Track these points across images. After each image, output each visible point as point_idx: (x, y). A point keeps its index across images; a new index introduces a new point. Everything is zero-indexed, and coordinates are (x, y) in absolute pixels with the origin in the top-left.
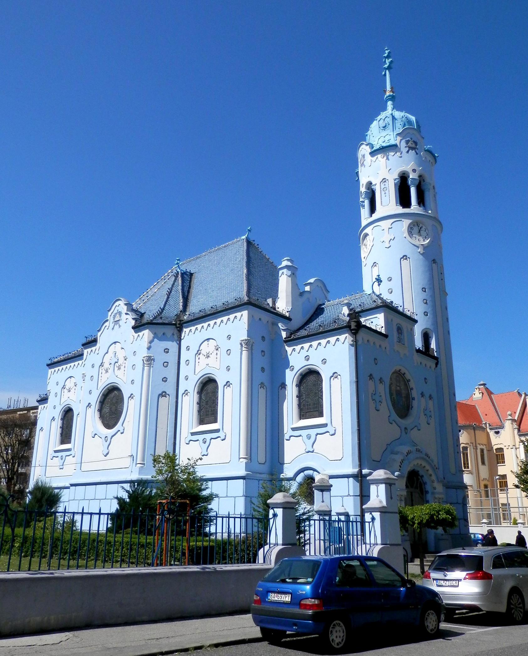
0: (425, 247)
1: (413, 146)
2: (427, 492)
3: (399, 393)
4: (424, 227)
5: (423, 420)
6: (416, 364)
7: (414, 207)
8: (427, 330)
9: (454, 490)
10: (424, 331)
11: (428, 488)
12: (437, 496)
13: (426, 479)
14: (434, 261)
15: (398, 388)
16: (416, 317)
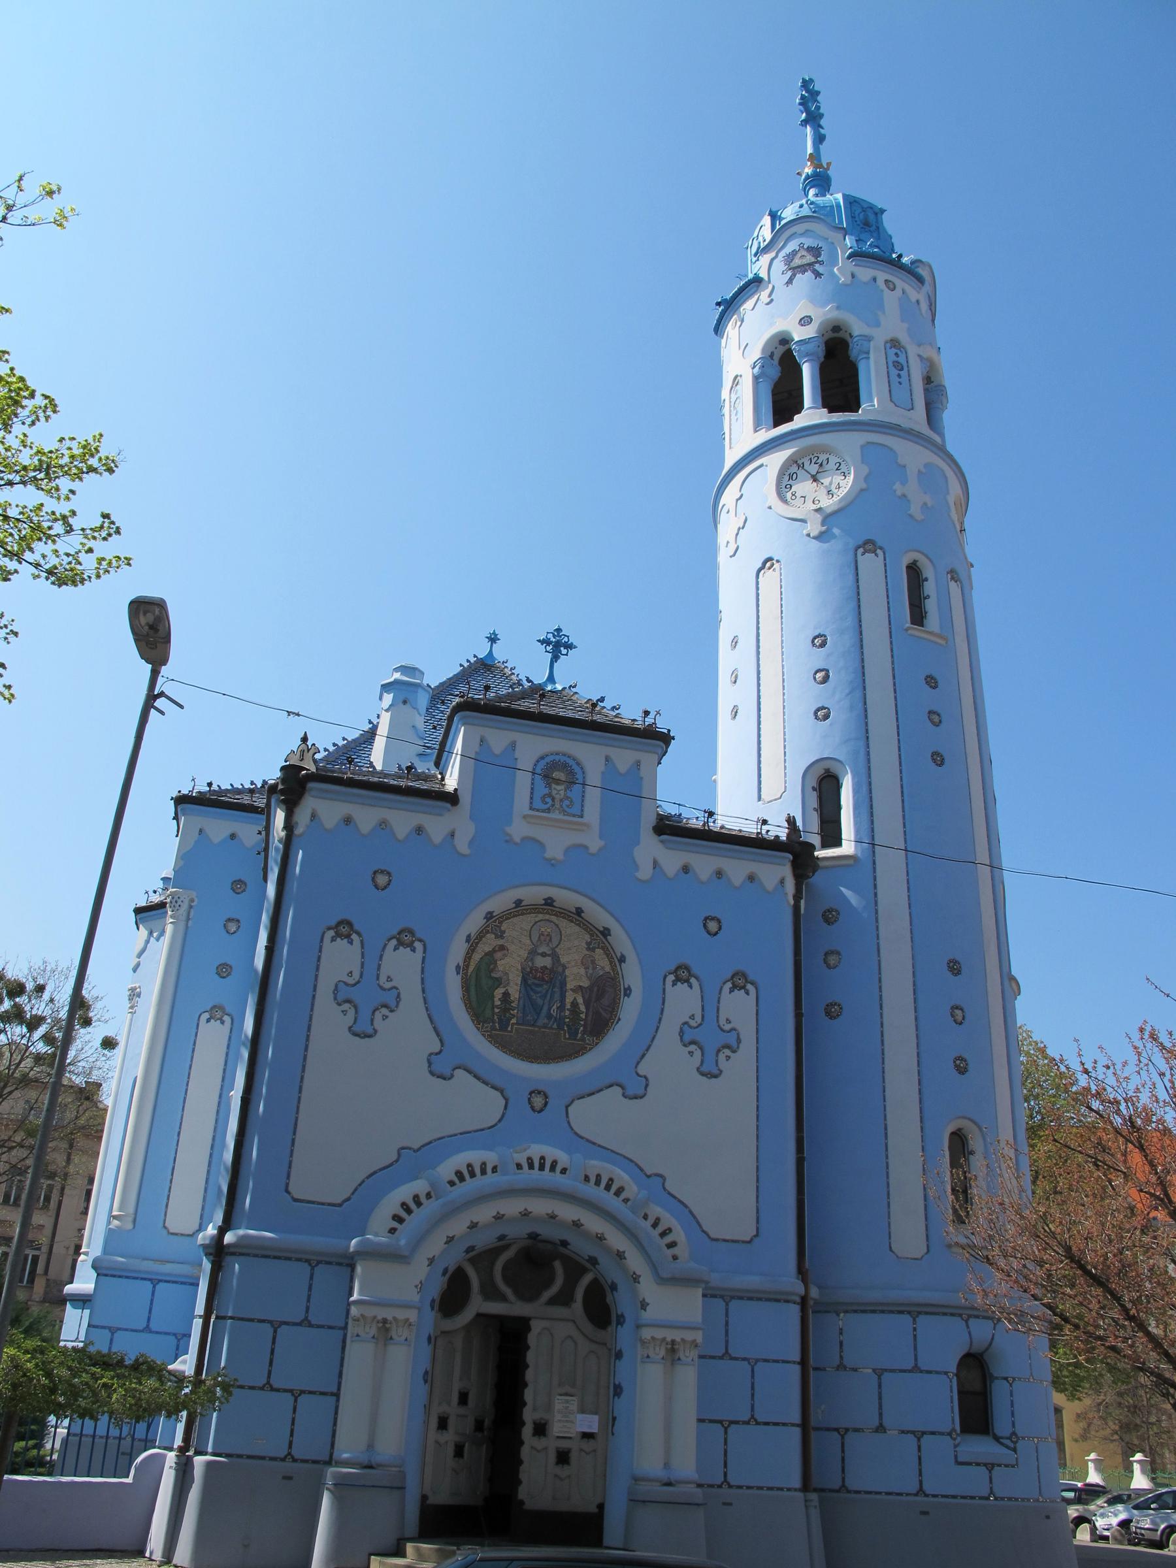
0: (828, 518)
1: (809, 258)
2: (621, 1320)
3: (543, 980)
4: (833, 459)
5: (669, 1062)
6: (645, 872)
7: (811, 414)
8: (827, 764)
9: (907, 1319)
10: (819, 771)
11: (622, 1302)
12: (647, 1334)
13: (609, 1270)
14: (869, 546)
15: (540, 962)
16: (662, 725)
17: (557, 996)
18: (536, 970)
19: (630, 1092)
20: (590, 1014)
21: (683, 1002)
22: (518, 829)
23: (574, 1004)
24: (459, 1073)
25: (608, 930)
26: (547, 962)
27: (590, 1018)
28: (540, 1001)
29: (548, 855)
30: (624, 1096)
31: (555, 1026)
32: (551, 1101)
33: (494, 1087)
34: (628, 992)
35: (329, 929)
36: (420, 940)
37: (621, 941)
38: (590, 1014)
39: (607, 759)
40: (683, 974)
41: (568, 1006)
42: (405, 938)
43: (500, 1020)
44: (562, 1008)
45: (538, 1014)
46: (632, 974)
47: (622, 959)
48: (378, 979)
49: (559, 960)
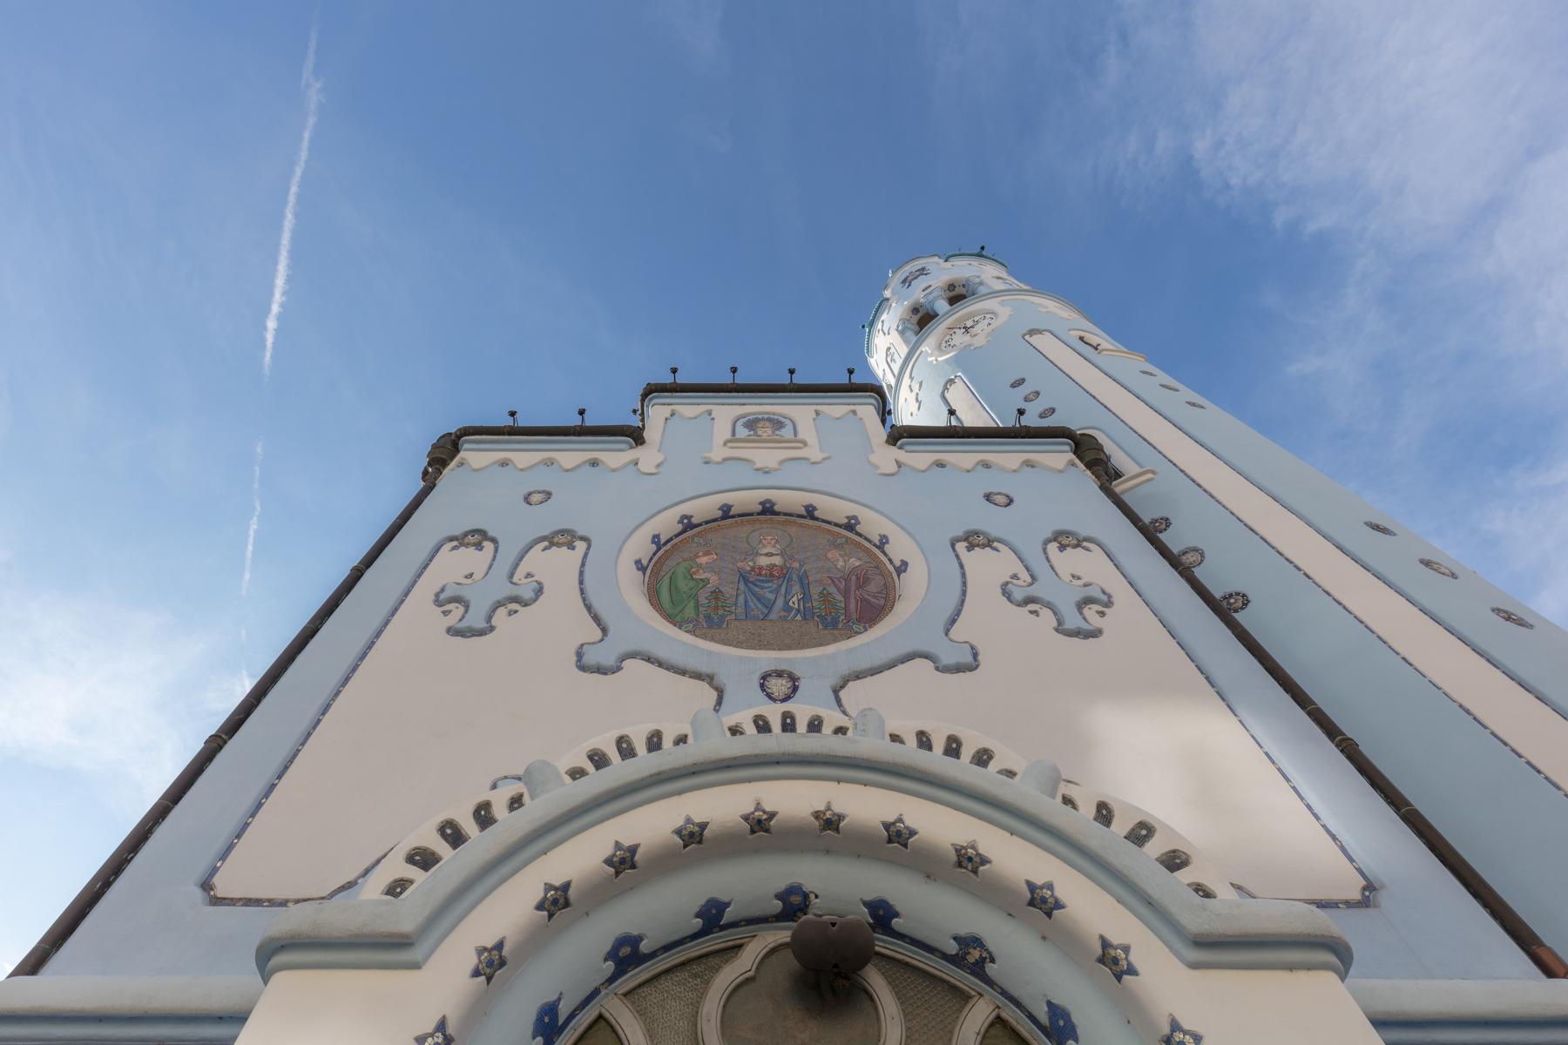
17: (796, 588)
18: (761, 568)
19: (948, 659)
20: (853, 601)
21: (988, 568)
22: (718, 453)
23: (825, 597)
24: (627, 663)
25: (855, 518)
26: (777, 560)
27: (852, 606)
28: (771, 596)
29: (758, 465)
30: (937, 669)
31: (799, 617)
32: (802, 684)
33: (698, 676)
34: (902, 568)
35: (451, 539)
36: (583, 539)
37: (873, 524)
38: (853, 601)
39: (817, 413)
40: (975, 540)
41: (815, 597)
42: (562, 538)
43: (708, 618)
44: (806, 597)
45: (770, 609)
46: (901, 547)
47: (884, 540)
48: (512, 575)
49: (791, 557)
